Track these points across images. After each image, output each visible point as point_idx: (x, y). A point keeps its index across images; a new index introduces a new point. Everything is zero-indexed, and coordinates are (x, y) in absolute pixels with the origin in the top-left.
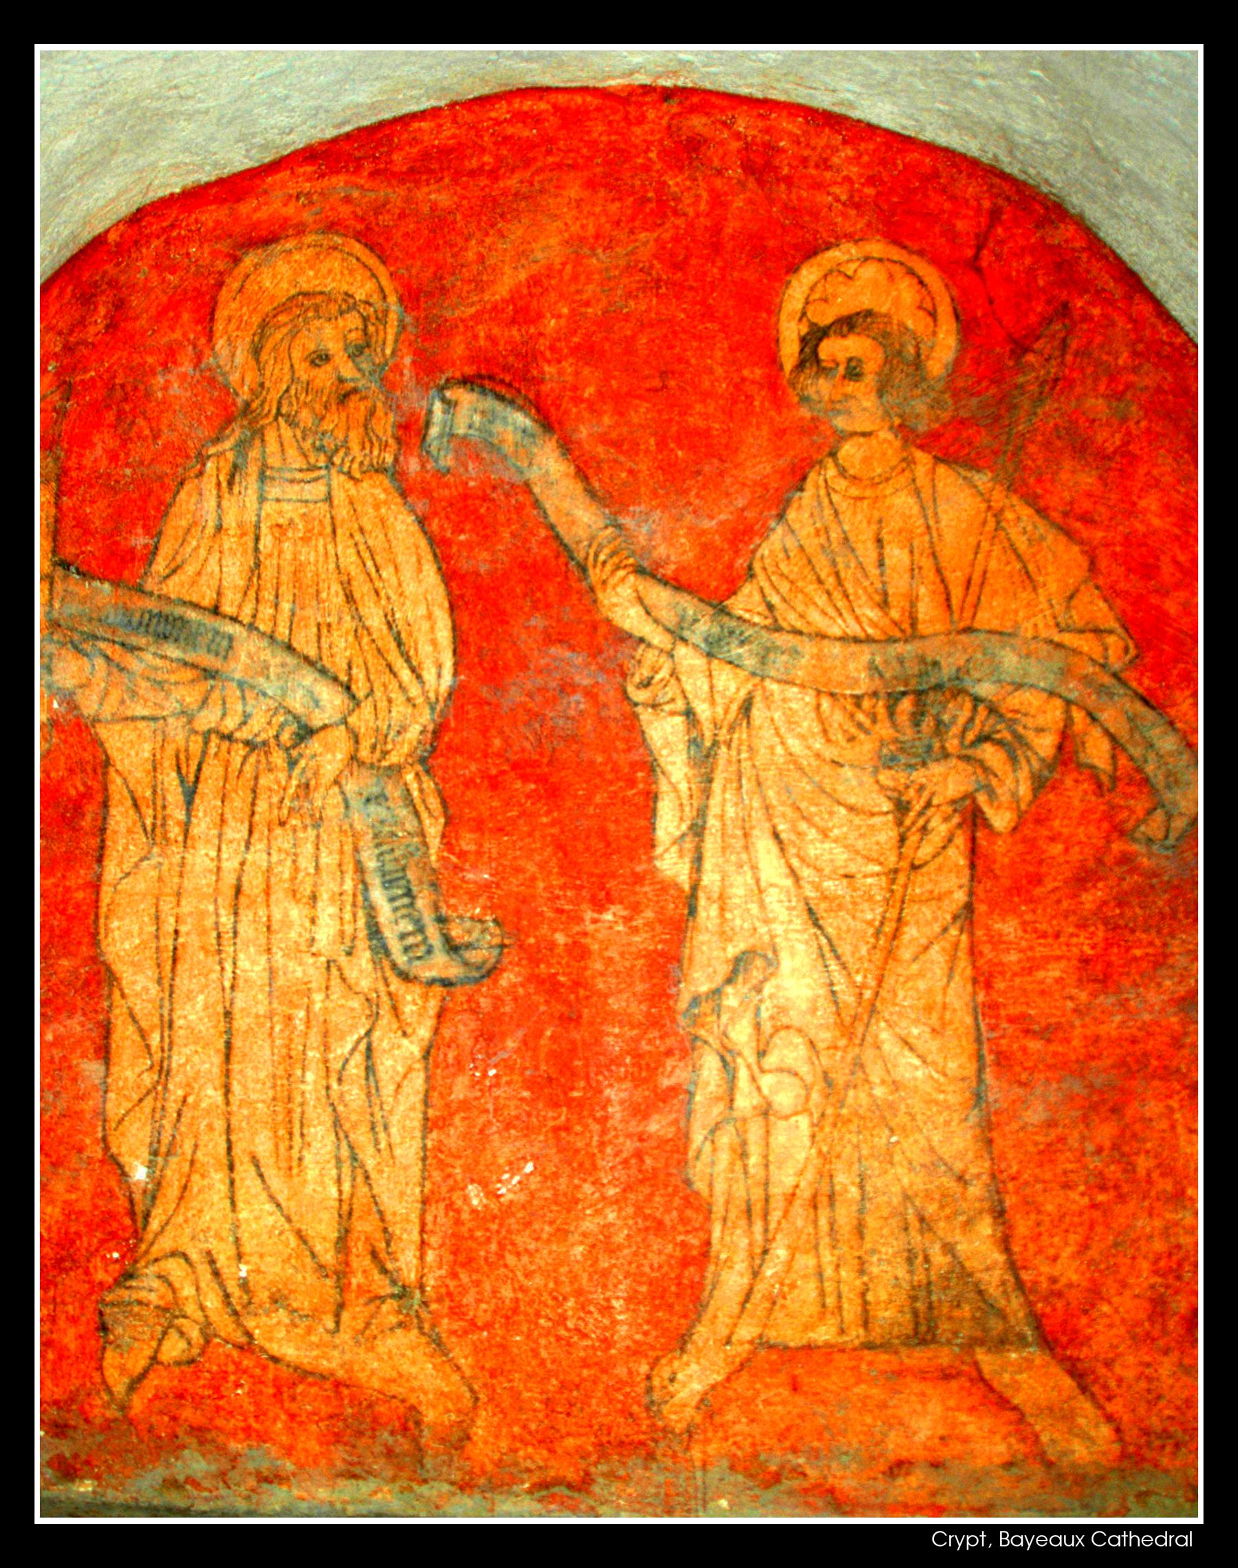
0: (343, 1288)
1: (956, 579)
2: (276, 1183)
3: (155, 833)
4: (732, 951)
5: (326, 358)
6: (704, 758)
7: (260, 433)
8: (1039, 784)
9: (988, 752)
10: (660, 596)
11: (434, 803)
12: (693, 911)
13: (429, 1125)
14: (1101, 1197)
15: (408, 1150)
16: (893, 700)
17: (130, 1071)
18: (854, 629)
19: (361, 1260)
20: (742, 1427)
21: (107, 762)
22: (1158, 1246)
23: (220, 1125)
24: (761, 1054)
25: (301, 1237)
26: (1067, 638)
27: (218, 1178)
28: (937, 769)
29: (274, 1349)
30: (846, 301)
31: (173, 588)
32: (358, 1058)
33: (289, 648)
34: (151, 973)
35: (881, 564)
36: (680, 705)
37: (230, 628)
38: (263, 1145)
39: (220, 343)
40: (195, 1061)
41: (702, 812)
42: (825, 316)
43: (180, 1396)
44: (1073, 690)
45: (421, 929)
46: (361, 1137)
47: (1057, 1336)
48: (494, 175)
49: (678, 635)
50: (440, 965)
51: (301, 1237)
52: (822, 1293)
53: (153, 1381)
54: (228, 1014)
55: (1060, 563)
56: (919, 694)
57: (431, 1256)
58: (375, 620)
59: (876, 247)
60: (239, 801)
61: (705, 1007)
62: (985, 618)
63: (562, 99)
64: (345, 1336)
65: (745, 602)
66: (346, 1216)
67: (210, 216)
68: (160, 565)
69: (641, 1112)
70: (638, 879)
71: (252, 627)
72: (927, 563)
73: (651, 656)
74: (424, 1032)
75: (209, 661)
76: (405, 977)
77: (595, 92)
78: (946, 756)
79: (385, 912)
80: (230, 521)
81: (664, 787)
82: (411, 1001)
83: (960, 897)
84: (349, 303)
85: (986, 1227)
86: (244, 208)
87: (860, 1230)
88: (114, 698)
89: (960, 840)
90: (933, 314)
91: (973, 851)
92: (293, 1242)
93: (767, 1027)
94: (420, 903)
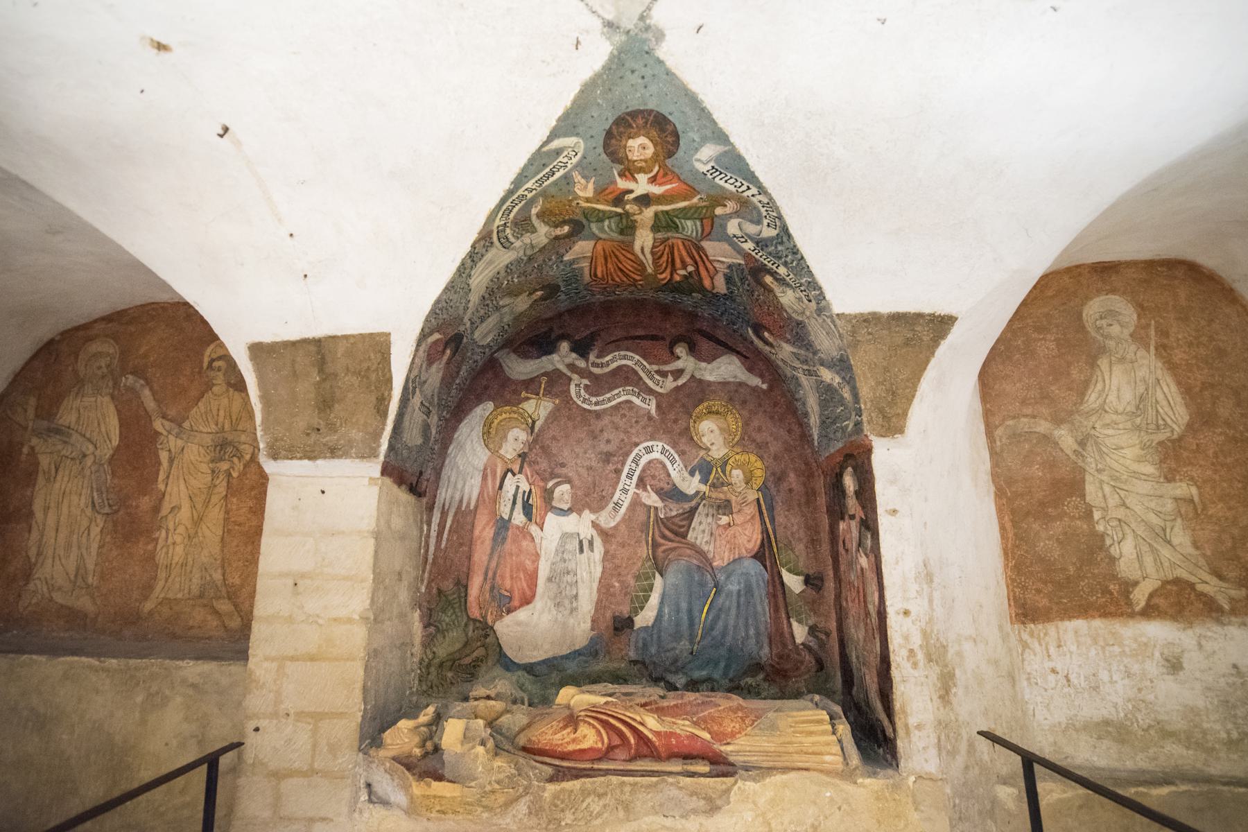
3: (48, 480)
6: (171, 461)
8: (245, 466)
10: (167, 423)
13: (100, 547)
17: (35, 535)
27: (50, 561)
31: (61, 422)
38: (62, 553)
40: (50, 533)
49: (169, 432)
50: (107, 510)
58: (103, 430)
60: (67, 473)
62: (240, 427)
65: (186, 425)
66: (78, 569)
67: (81, 333)
69: (148, 544)
82: (99, 517)
84: (108, 354)
85: (220, 571)
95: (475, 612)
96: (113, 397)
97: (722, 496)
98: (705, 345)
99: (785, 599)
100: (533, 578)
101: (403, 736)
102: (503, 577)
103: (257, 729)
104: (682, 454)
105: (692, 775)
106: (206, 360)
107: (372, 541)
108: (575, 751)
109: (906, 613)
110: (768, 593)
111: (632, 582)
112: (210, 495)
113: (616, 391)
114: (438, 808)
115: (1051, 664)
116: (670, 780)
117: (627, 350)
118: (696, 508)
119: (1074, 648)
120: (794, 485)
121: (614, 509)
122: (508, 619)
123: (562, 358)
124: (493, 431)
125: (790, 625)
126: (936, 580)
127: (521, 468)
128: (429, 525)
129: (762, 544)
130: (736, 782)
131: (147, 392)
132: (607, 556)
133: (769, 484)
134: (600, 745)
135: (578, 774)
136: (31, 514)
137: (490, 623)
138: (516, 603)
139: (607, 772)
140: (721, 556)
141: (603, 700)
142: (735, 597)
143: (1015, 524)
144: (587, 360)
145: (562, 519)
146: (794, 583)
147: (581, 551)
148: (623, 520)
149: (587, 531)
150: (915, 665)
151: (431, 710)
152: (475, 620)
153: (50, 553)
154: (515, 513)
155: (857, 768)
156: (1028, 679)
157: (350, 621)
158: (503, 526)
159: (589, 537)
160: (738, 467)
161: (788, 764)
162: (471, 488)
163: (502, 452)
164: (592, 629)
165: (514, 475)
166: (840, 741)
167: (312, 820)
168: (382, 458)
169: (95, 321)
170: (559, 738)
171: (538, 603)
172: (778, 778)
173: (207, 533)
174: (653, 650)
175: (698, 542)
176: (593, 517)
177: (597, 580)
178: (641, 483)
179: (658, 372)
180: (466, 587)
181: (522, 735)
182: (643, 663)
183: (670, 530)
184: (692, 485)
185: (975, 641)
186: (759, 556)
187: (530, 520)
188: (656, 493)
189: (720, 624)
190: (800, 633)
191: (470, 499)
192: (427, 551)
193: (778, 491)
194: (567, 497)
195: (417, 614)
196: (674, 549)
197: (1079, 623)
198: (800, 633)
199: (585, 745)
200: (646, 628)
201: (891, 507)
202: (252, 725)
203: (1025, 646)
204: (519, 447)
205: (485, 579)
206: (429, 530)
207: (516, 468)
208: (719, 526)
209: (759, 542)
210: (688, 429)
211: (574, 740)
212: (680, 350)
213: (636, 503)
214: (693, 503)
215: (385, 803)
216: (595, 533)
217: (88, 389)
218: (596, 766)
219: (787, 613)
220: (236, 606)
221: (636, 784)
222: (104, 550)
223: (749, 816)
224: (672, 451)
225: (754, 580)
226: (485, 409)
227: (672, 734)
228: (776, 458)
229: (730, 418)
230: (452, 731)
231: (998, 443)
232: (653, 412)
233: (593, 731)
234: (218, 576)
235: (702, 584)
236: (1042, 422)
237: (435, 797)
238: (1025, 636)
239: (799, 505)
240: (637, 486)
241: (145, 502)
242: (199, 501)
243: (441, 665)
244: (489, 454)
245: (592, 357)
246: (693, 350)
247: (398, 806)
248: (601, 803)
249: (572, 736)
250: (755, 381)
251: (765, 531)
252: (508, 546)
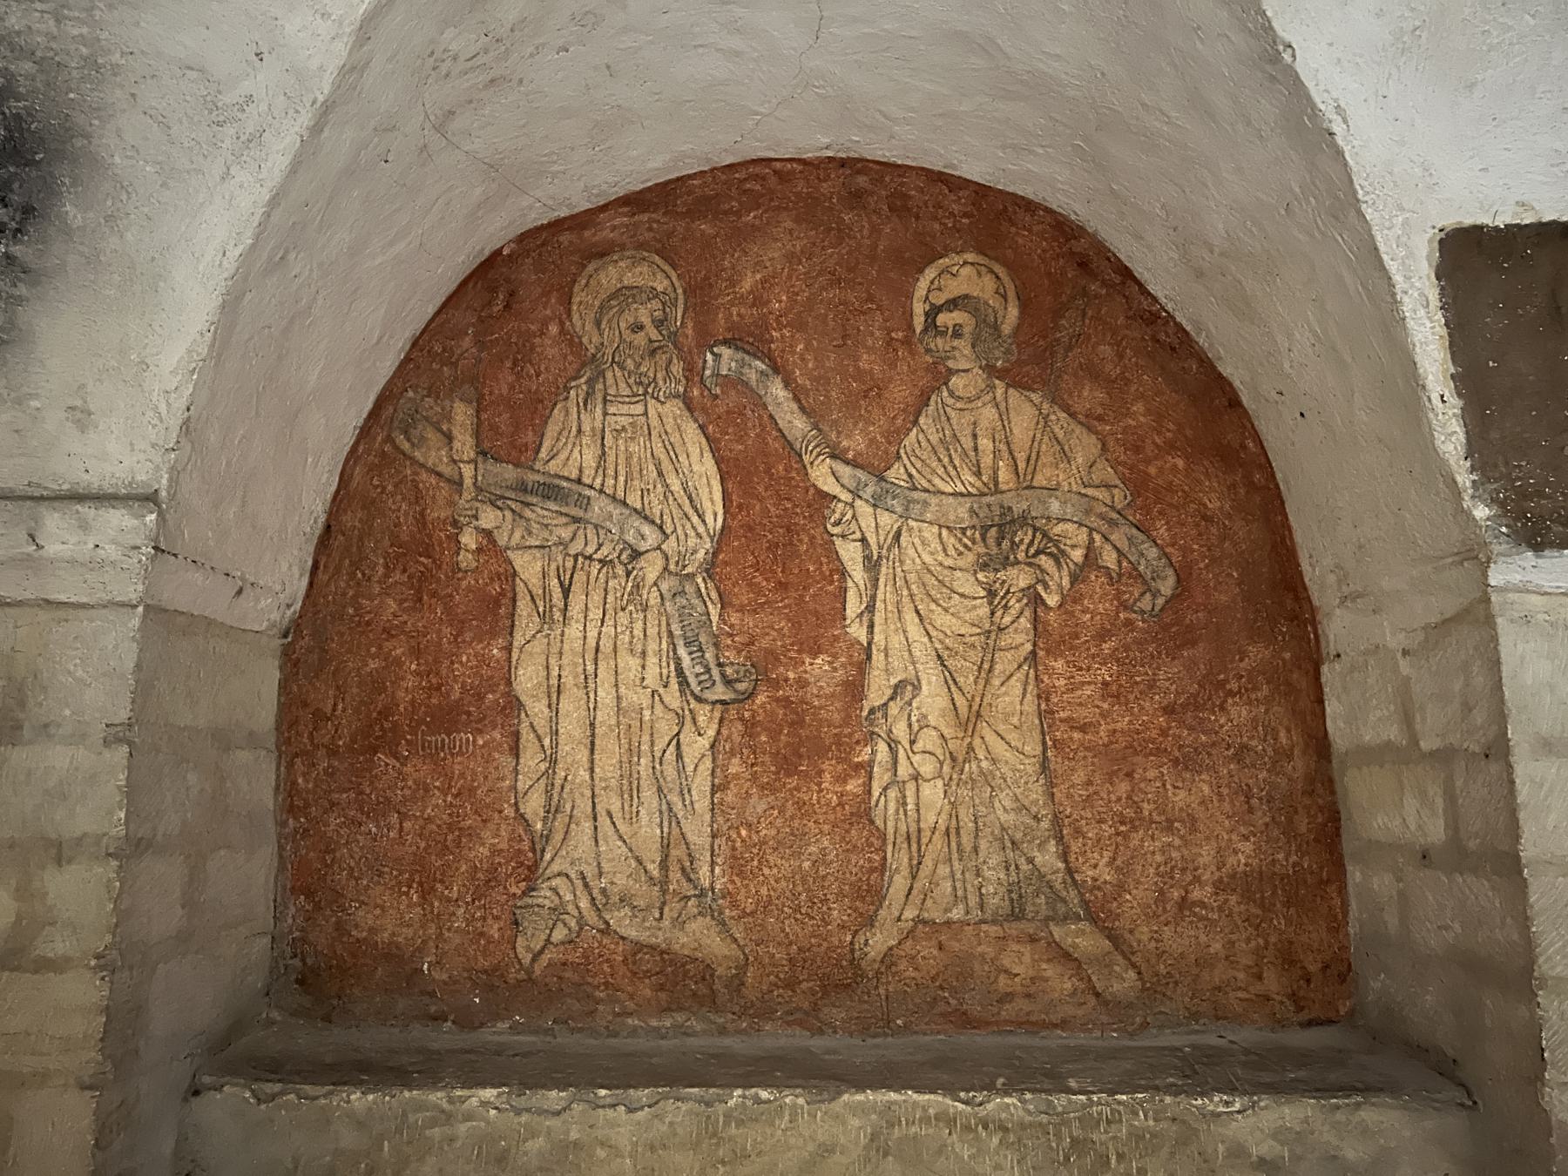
0: (664, 892)
1: (1021, 457)
2: (622, 828)
3: (545, 618)
4: (893, 681)
5: (641, 328)
6: (872, 565)
7: (602, 374)
8: (1074, 579)
9: (1043, 560)
10: (845, 471)
11: (714, 595)
12: (869, 657)
14: (1123, 828)
15: (702, 805)
16: (985, 530)
17: (531, 760)
18: (960, 488)
19: (675, 875)
20: (911, 973)
21: (515, 574)
22: (1159, 858)
23: (588, 793)
24: (912, 742)
25: (639, 862)
26: (1090, 491)
27: (587, 825)
28: (1012, 572)
29: (622, 932)
30: (954, 288)
31: (553, 467)
32: (672, 748)
33: (624, 503)
34: (545, 702)
35: (976, 449)
36: (858, 535)
37: (588, 492)
38: (615, 807)
39: (576, 317)
40: (573, 752)
41: (873, 598)
42: (939, 299)
43: (564, 964)
44: (1093, 521)
45: (708, 671)
46: (674, 798)
47: (1097, 914)
48: (738, 214)
50: (720, 692)
51: (639, 862)
52: (955, 889)
53: (546, 956)
54: (592, 725)
55: (1084, 447)
56: (1000, 526)
57: (717, 870)
58: (676, 486)
59: (970, 257)
60: (596, 597)
61: (879, 715)
62: (1039, 480)
63: (778, 165)
64: (666, 923)
65: (896, 474)
66: (666, 847)
67: (565, 238)
68: (543, 454)
69: (842, 779)
70: (836, 638)
71: (601, 491)
72: (1003, 447)
73: (840, 505)
74: (711, 733)
75: (579, 513)
76: (699, 700)
77: (799, 161)
78: (1018, 563)
79: (686, 661)
80: (586, 427)
81: (850, 584)
82: (703, 713)
83: (1029, 647)
84: (654, 294)
85: (1052, 846)
86: (587, 234)
87: (976, 849)
88: (517, 535)
89: (1027, 613)
90: (1005, 297)
91: (1035, 620)
92: (634, 864)
93: (916, 727)
94: (707, 655)
96: (689, 406)
106: (919, 309)
112: (990, 651)
131: (777, 391)
136: (513, 705)
153: (584, 806)
169: (604, 208)
173: (999, 747)
217: (615, 381)
220: (1114, 938)
222: (730, 797)
234: (1048, 858)
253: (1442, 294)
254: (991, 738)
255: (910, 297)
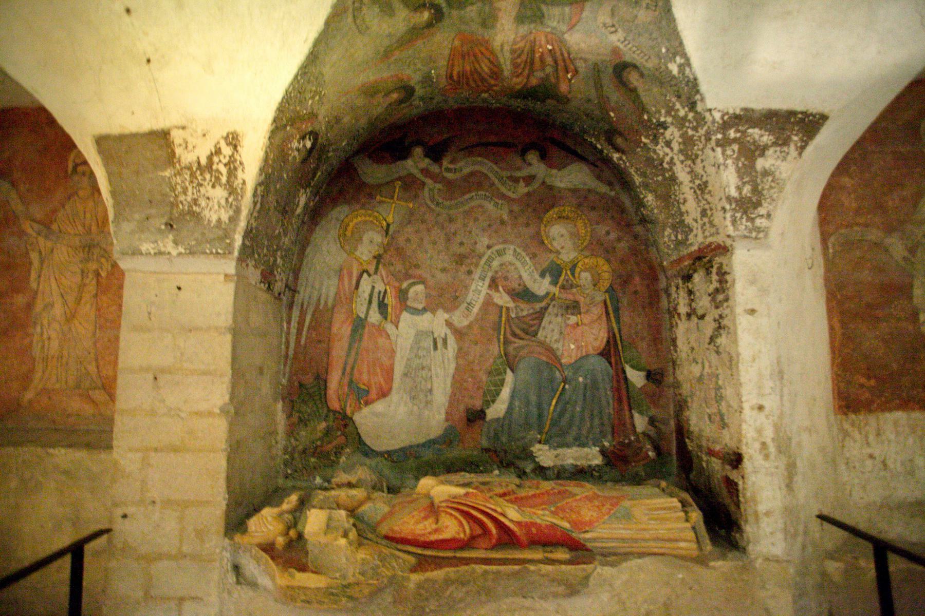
6: (42, 262)
9: (103, 260)
10: (36, 226)
49: (39, 233)
65: (54, 227)
85: (94, 364)
87: (67, 364)
91: (98, 282)
95: (335, 404)
97: (571, 297)
98: (556, 154)
99: (628, 391)
100: (389, 373)
101: (266, 524)
102: (361, 373)
103: (125, 516)
104: (534, 256)
105: (552, 562)
107: (229, 337)
108: (437, 541)
109: (761, 408)
110: (612, 388)
111: (484, 378)
113: (467, 196)
114: (303, 598)
115: (869, 451)
116: (532, 568)
117: (480, 155)
118: (546, 308)
119: (892, 437)
120: (638, 288)
121: (467, 308)
122: (366, 411)
123: (415, 163)
124: (348, 234)
125: (632, 417)
126: (785, 377)
127: (377, 269)
128: (289, 323)
129: (608, 342)
130: (595, 568)
131: (14, 195)
132: (461, 353)
133: (615, 287)
134: (462, 536)
135: (438, 563)
137: (349, 411)
138: (373, 395)
139: (467, 561)
140: (569, 351)
141: (461, 491)
142: (581, 392)
143: (844, 324)
144: (441, 167)
145: (417, 318)
146: (636, 378)
147: (436, 348)
148: (476, 320)
149: (441, 330)
150: (767, 457)
151: (294, 498)
152: (335, 412)
154: (371, 312)
155: (710, 553)
156: (847, 464)
157: (210, 414)
158: (359, 325)
159: (443, 335)
160: (586, 270)
161: (644, 550)
162: (329, 289)
163: (358, 253)
164: (447, 420)
165: (369, 275)
166: (694, 528)
167: (182, 600)
168: (236, 253)
170: (422, 528)
171: (394, 397)
172: (635, 562)
174: (504, 439)
175: (548, 340)
176: (446, 316)
177: (451, 375)
178: (494, 284)
179: (510, 178)
180: (326, 381)
181: (384, 524)
182: (495, 451)
183: (517, 328)
184: (542, 286)
185: (810, 431)
186: (605, 353)
187: (386, 318)
188: (508, 293)
189: (567, 415)
190: (640, 422)
191: (327, 299)
192: (287, 348)
193: (624, 292)
194: (422, 296)
195: (280, 405)
196: (527, 345)
197: (900, 415)
198: (640, 422)
199: (447, 535)
200: (498, 420)
201: (749, 307)
202: (119, 512)
203: (846, 434)
204: (375, 250)
205: (343, 373)
206: (289, 328)
207: (372, 271)
208: (567, 325)
209: (605, 340)
210: (538, 233)
211: (436, 531)
212: (532, 157)
213: (488, 303)
214: (543, 304)
215: (254, 585)
216: (449, 332)
218: (458, 554)
219: (629, 405)
221: (499, 572)
223: (605, 597)
224: (524, 254)
225: (599, 377)
226: (340, 212)
227: (534, 524)
228: (622, 261)
229: (580, 223)
230: (314, 522)
231: (831, 251)
232: (505, 217)
233: (455, 522)
234: (92, 368)
235: (552, 380)
236: (874, 231)
237: (299, 588)
238: (847, 426)
239: (643, 308)
240: (490, 286)
241: (20, 300)
242: (71, 298)
243: (304, 451)
244: (345, 255)
245: (445, 163)
246: (543, 157)
247: (265, 589)
248: (464, 590)
249: (434, 526)
250: (603, 189)
251: (610, 330)
252: (366, 342)
253: (103, 159)
254: (77, 324)
255: (67, 160)
